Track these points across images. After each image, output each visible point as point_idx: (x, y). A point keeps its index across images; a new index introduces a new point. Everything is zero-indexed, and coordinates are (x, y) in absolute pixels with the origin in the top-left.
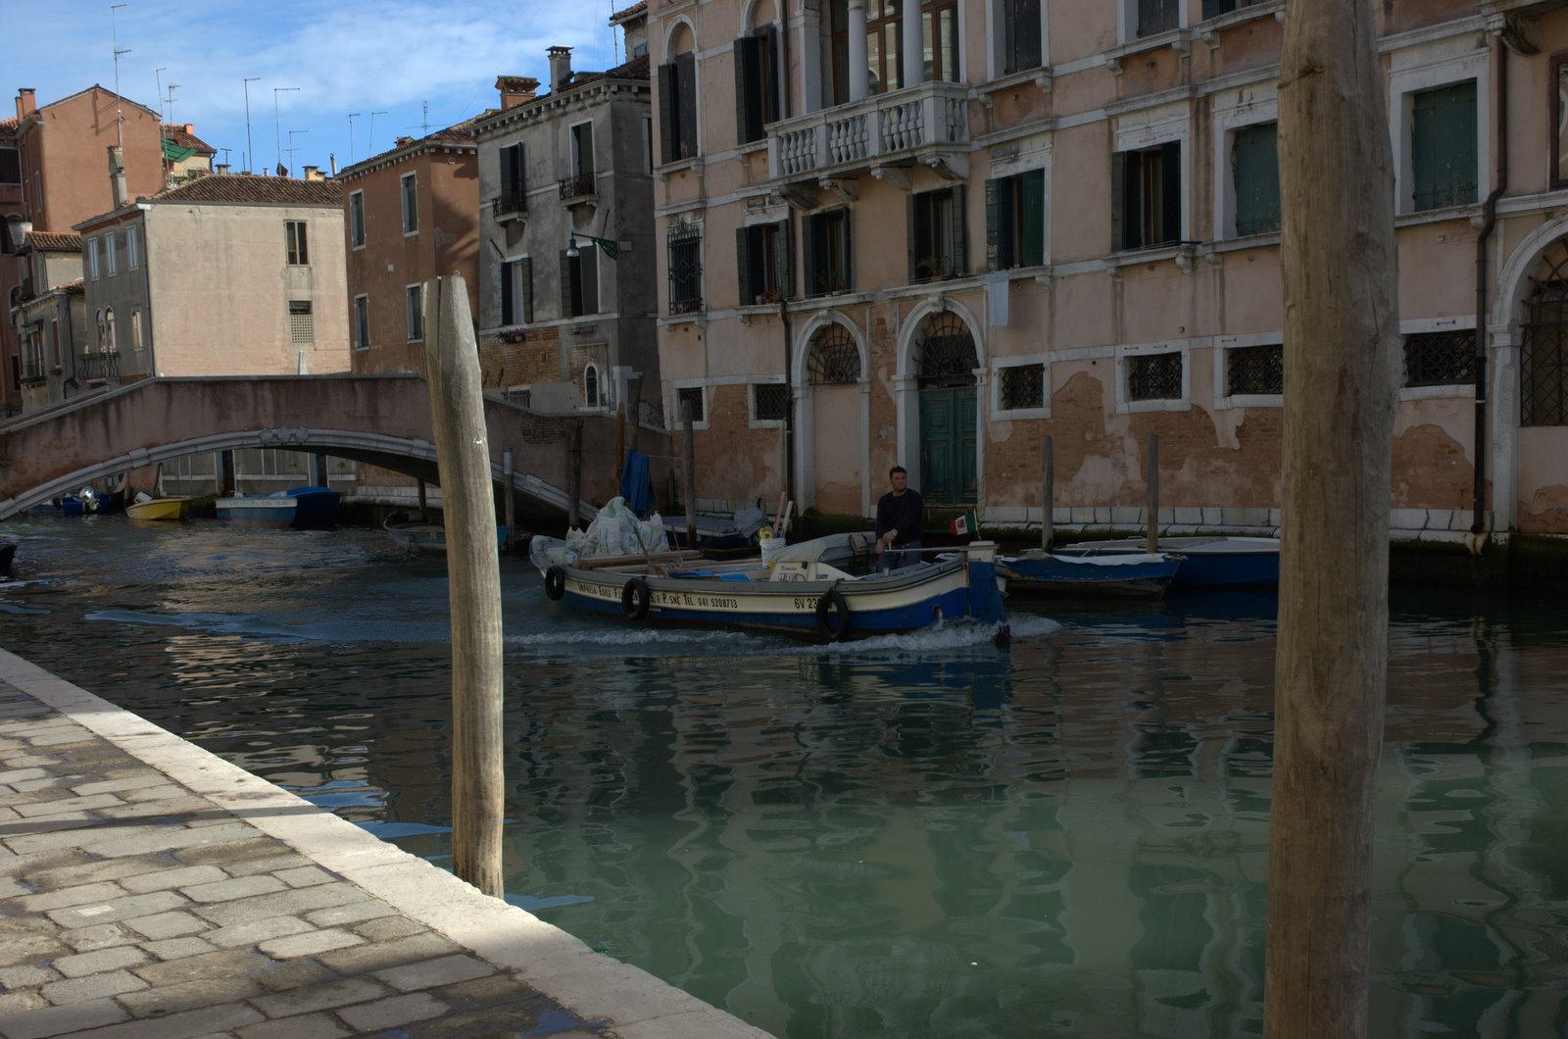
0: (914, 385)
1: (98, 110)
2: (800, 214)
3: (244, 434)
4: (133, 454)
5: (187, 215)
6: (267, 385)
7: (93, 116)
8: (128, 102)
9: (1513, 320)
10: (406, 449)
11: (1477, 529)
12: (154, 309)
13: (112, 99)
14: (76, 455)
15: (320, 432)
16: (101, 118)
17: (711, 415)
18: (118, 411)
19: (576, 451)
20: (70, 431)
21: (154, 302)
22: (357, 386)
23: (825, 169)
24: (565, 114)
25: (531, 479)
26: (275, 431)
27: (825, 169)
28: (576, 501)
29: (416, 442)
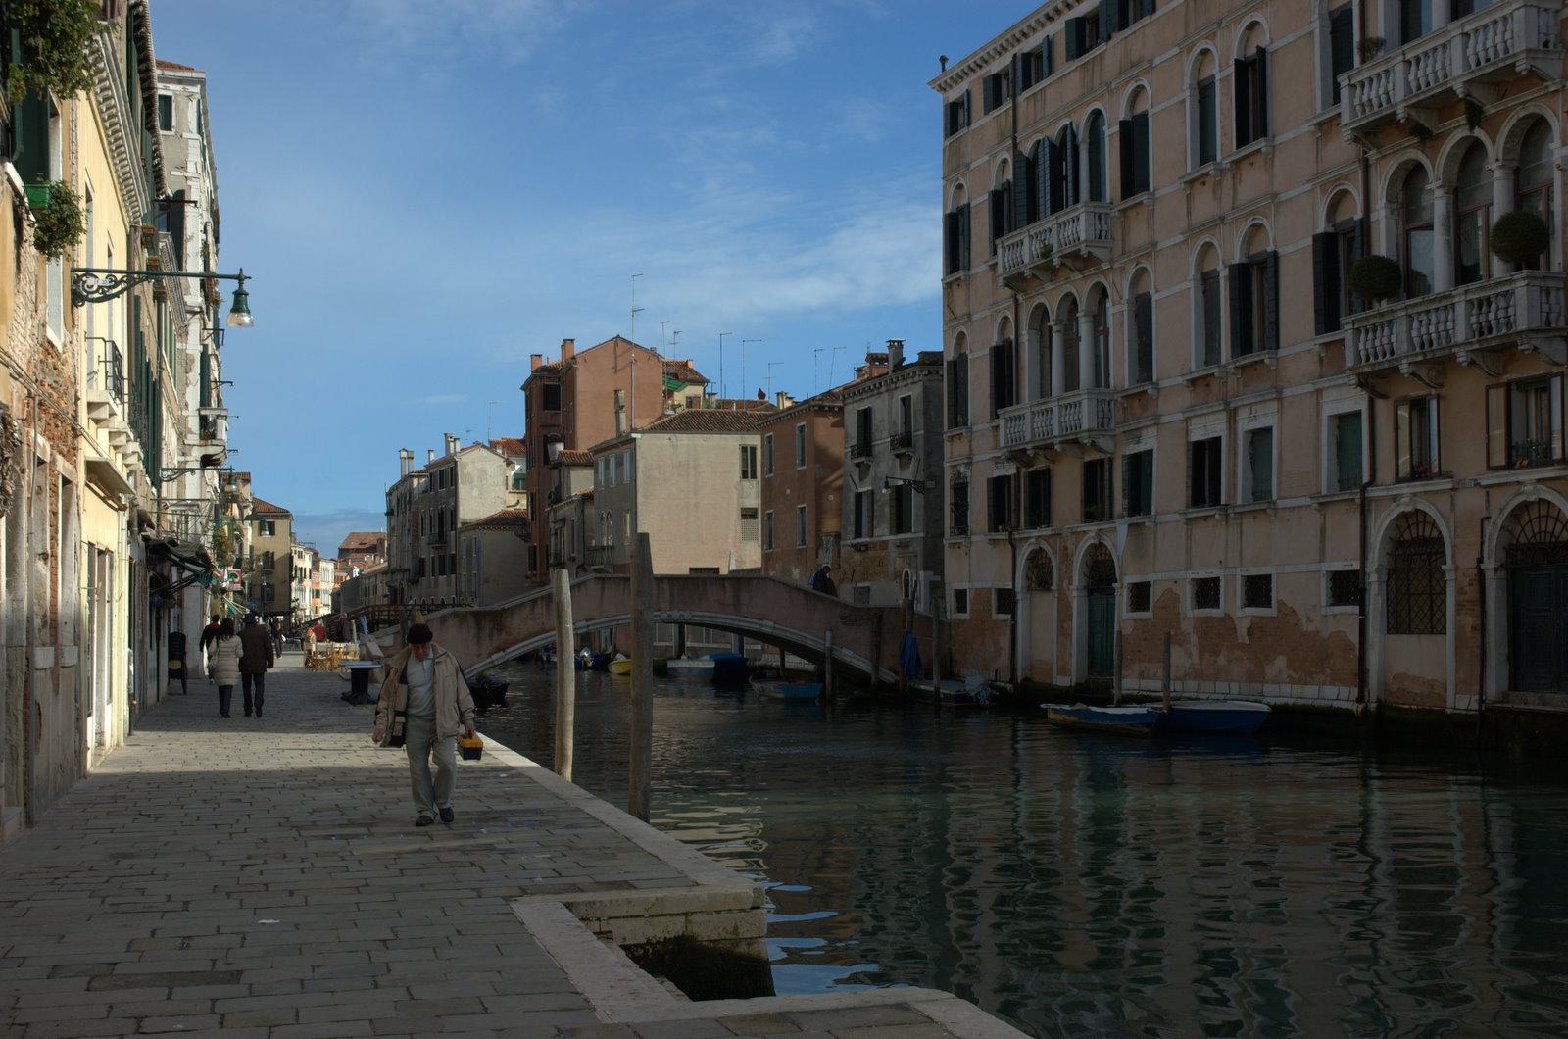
0: (1085, 593)
1: (618, 354)
2: (1023, 470)
5: (667, 442)
6: (666, 581)
7: (613, 360)
9: (1379, 565)
10: (758, 627)
11: (1360, 700)
12: (639, 514)
14: (543, 624)
15: (700, 613)
16: (620, 360)
17: (972, 609)
19: (878, 632)
21: (639, 507)
22: (726, 582)
23: (1030, 442)
24: (896, 388)
25: (845, 651)
26: (670, 612)
27: (1030, 442)
28: (876, 668)
29: (765, 622)
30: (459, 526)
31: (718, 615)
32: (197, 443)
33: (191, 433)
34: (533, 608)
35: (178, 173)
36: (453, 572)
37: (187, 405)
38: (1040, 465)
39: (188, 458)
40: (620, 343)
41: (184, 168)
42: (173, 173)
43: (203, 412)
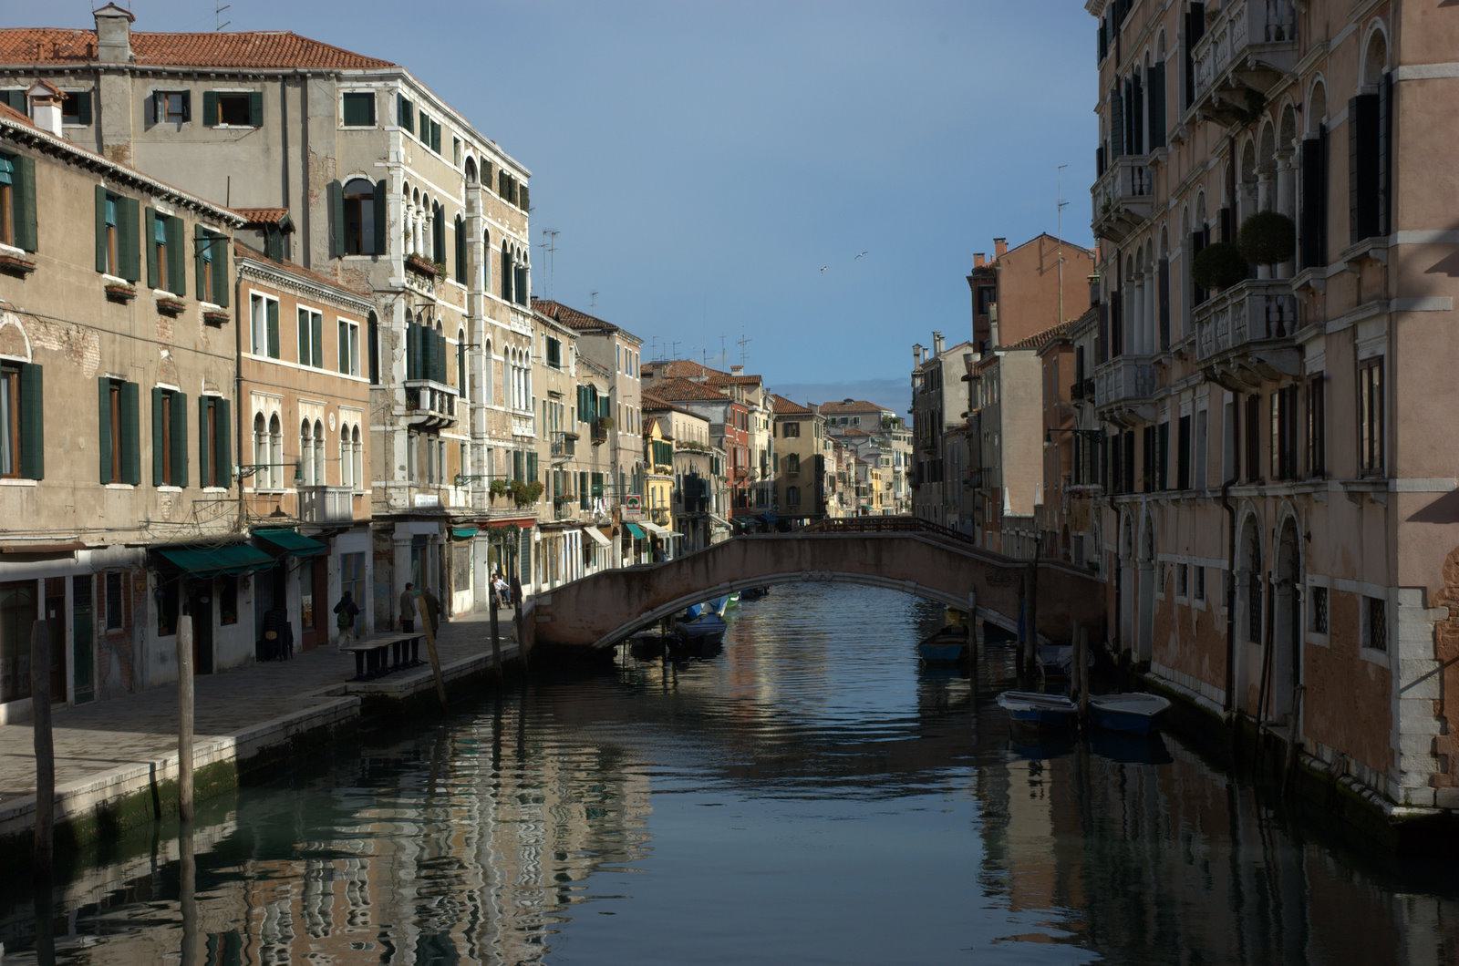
1: (1044, 252)
6: (807, 542)
8: (1068, 244)
9: (1242, 568)
11: (1228, 707)
12: (1004, 436)
13: (1056, 244)
15: (841, 574)
18: (714, 555)
20: (686, 569)
21: (1004, 429)
22: (867, 543)
30: (945, 430)
33: (398, 404)
36: (942, 480)
37: (393, 379)
38: (1130, 428)
39: (395, 428)
40: (1046, 241)
41: (386, 159)
42: (377, 164)
43: (408, 385)
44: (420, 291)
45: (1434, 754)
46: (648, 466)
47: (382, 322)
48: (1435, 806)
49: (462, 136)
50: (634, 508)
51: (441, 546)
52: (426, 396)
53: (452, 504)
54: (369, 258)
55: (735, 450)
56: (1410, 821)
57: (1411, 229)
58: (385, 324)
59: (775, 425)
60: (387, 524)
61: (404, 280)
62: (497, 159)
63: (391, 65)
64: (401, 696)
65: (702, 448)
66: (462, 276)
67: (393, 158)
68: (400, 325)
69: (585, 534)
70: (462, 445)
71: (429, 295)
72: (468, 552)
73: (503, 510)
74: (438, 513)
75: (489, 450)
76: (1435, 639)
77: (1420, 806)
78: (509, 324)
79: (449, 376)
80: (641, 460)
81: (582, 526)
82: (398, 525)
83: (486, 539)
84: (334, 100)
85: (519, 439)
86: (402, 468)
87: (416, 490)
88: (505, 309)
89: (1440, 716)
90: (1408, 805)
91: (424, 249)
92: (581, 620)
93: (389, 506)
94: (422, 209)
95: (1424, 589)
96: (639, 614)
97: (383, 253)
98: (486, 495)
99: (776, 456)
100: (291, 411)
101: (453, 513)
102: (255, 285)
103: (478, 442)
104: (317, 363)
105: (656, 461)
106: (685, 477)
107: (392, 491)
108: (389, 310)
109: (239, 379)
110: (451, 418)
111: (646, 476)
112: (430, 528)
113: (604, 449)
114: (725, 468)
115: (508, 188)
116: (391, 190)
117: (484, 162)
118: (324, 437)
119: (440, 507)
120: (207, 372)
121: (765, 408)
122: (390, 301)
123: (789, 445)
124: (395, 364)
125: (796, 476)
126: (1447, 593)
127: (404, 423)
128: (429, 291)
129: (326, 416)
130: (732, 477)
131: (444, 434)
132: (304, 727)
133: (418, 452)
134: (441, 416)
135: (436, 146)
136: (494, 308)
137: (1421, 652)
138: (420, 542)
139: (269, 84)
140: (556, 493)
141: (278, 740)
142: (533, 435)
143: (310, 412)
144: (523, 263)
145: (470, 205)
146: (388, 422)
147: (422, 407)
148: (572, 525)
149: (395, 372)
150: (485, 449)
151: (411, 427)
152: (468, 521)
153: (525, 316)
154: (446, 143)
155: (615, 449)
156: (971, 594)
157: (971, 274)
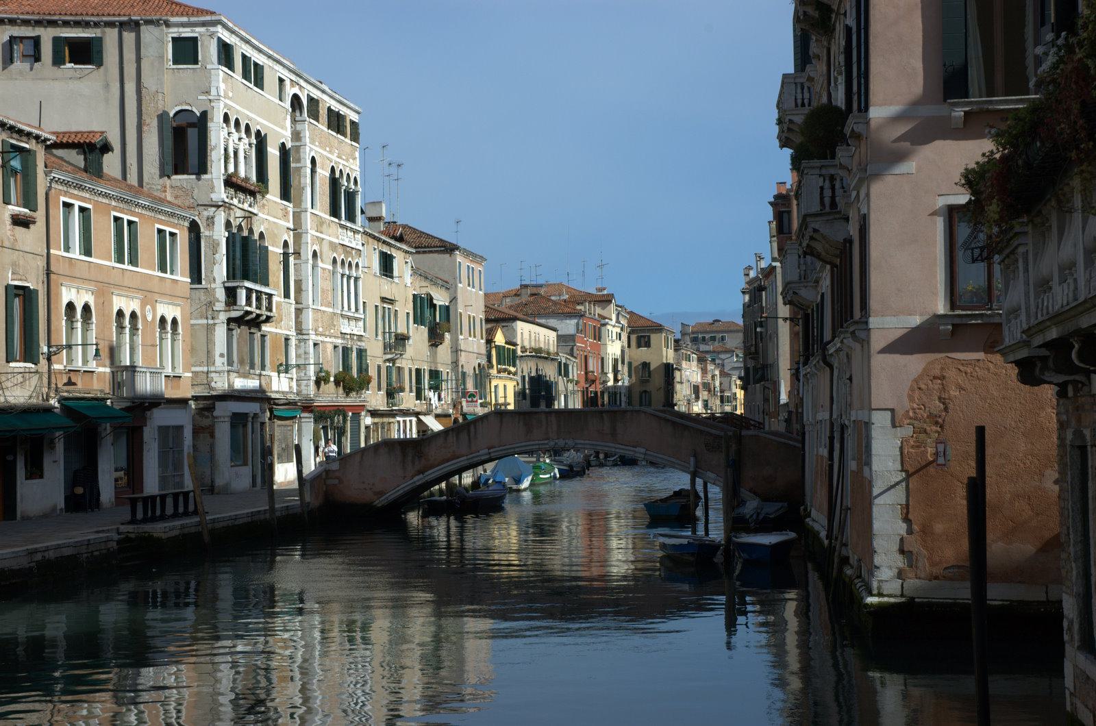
3: (540, 442)
4: (481, 452)
6: (553, 415)
10: (632, 453)
15: (582, 442)
29: (637, 449)
31: (598, 443)
32: (223, 309)
33: (218, 301)
34: (446, 439)
35: (204, 98)
37: (214, 280)
39: (216, 321)
41: (208, 92)
42: (199, 97)
43: (226, 285)
44: (240, 206)
45: (902, 551)
46: (490, 366)
47: (204, 232)
48: (902, 595)
49: (285, 74)
50: (472, 401)
51: (263, 424)
52: (242, 294)
53: (275, 387)
54: (194, 177)
55: (586, 357)
56: (881, 608)
57: (881, 105)
58: (207, 233)
59: (629, 338)
60: (210, 403)
61: (224, 196)
62: (325, 97)
63: (213, 13)
64: (164, 536)
65: (548, 353)
66: (285, 194)
67: (213, 92)
68: (220, 234)
69: (420, 422)
70: (287, 339)
71: (250, 209)
72: (292, 430)
73: (331, 395)
74: (259, 395)
75: (315, 345)
76: (902, 454)
77: (889, 596)
78: (338, 238)
79: (271, 279)
80: (484, 362)
81: (417, 414)
82: (218, 404)
83: (312, 420)
84: (162, 42)
85: (349, 337)
86: (222, 355)
87: (235, 374)
88: (333, 225)
89: (906, 519)
90: (880, 595)
91: (246, 171)
92: (363, 483)
93: (211, 388)
94: (243, 135)
95: (892, 411)
96: (413, 477)
97: (205, 172)
98: (312, 384)
99: (630, 364)
100: (104, 303)
101: (273, 396)
102: (66, 194)
103: (305, 337)
104: (134, 261)
105: (499, 363)
106: (531, 378)
107: (213, 375)
108: (211, 221)
109: (48, 272)
110: (269, 314)
111: (489, 375)
112: (251, 408)
113: (444, 350)
114: (575, 372)
115: (336, 122)
116: (212, 120)
117: (311, 100)
118: (140, 326)
119: (261, 390)
120: (14, 265)
121: (618, 321)
122: (211, 214)
123: (642, 355)
124: (216, 267)
125: (648, 381)
126: (911, 414)
127: (223, 317)
128: (250, 206)
129: (143, 307)
130: (583, 380)
131: (266, 328)
132: (51, 555)
133: (238, 343)
134: (258, 312)
135: (259, 83)
136: (320, 224)
137: (891, 464)
138: (239, 420)
139: (108, 30)
140: (389, 384)
141: (24, 563)
142: (363, 334)
143: (129, 305)
144: (353, 187)
145: (297, 136)
146: (209, 317)
147: (238, 304)
148: (405, 413)
149: (216, 274)
150: (311, 344)
151: (230, 320)
152: (290, 403)
153: (355, 232)
154: (270, 80)
155: (456, 351)
156: (692, 459)
157: (772, 200)
